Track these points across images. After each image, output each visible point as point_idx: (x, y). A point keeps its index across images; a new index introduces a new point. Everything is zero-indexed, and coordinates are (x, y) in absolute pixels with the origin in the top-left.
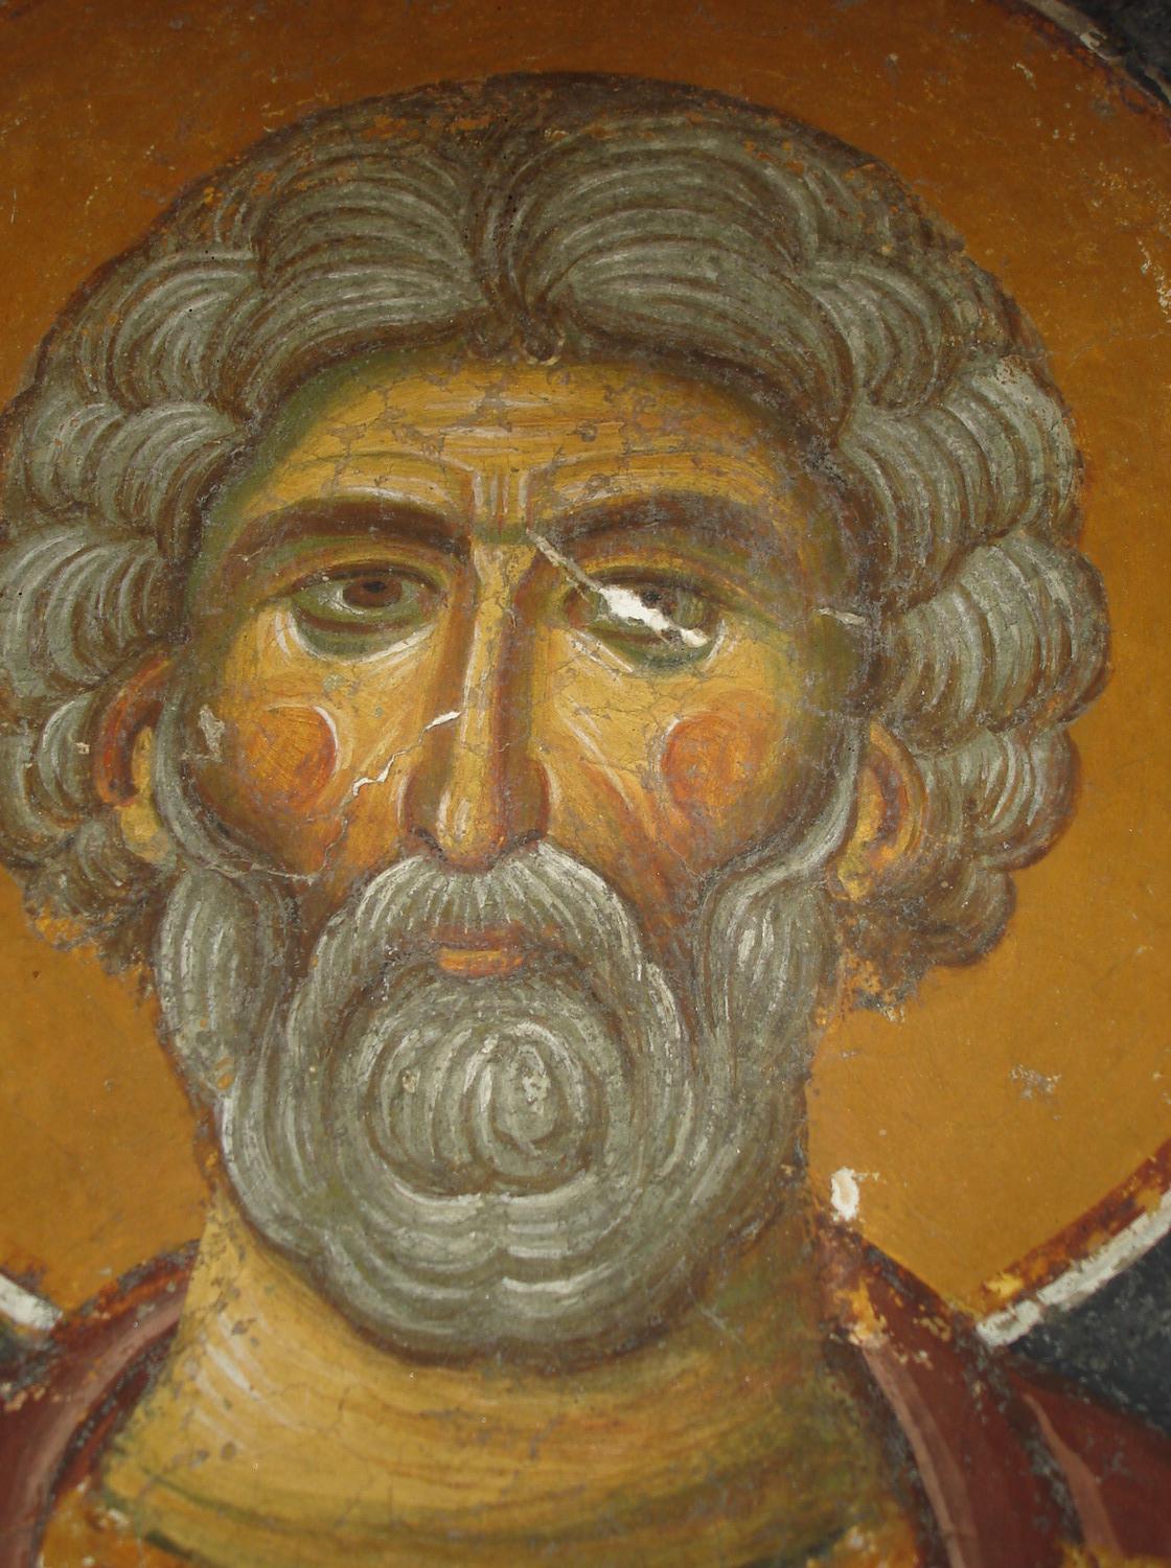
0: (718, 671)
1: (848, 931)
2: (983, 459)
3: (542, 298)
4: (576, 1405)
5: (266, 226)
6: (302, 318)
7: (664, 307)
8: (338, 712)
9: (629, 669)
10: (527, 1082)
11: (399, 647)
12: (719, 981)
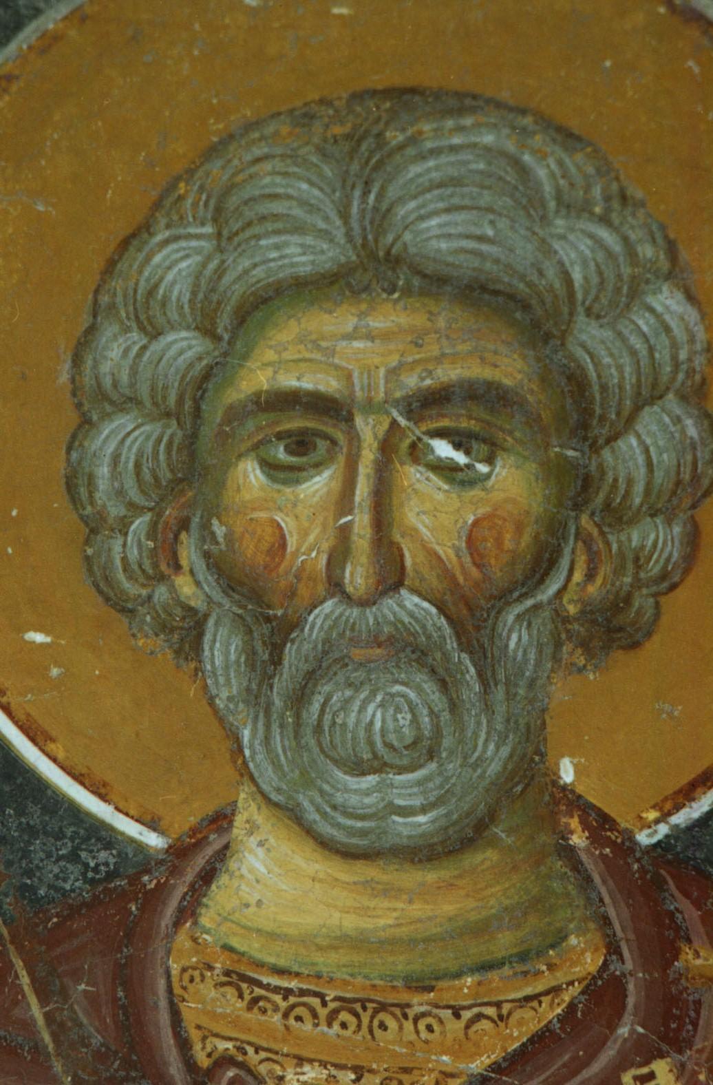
0: (496, 487)
1: (568, 631)
2: (651, 350)
3: (388, 253)
4: (431, 876)
5: (218, 210)
6: (246, 272)
7: (462, 257)
8: (287, 519)
9: (446, 487)
10: (399, 716)
11: (317, 479)
12: (499, 661)
